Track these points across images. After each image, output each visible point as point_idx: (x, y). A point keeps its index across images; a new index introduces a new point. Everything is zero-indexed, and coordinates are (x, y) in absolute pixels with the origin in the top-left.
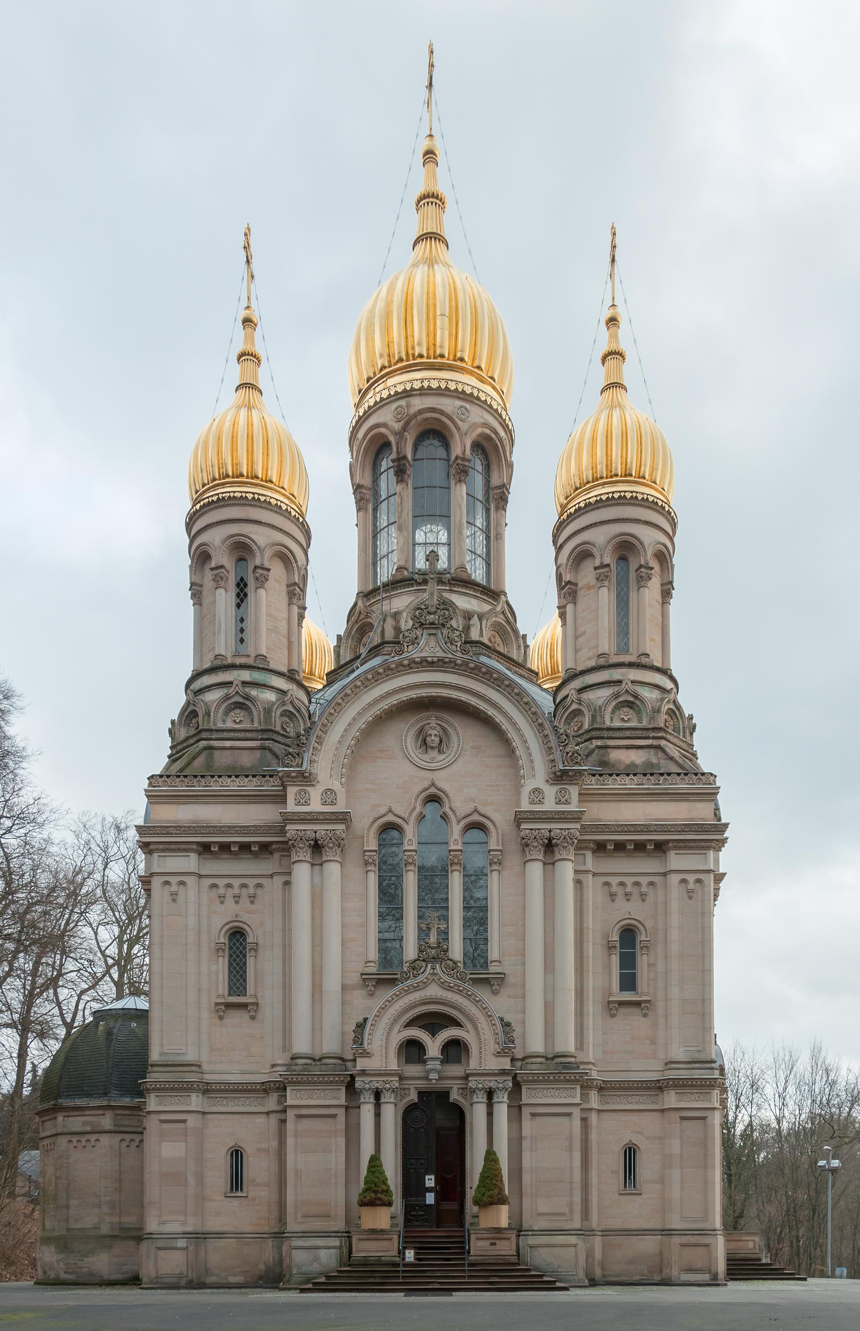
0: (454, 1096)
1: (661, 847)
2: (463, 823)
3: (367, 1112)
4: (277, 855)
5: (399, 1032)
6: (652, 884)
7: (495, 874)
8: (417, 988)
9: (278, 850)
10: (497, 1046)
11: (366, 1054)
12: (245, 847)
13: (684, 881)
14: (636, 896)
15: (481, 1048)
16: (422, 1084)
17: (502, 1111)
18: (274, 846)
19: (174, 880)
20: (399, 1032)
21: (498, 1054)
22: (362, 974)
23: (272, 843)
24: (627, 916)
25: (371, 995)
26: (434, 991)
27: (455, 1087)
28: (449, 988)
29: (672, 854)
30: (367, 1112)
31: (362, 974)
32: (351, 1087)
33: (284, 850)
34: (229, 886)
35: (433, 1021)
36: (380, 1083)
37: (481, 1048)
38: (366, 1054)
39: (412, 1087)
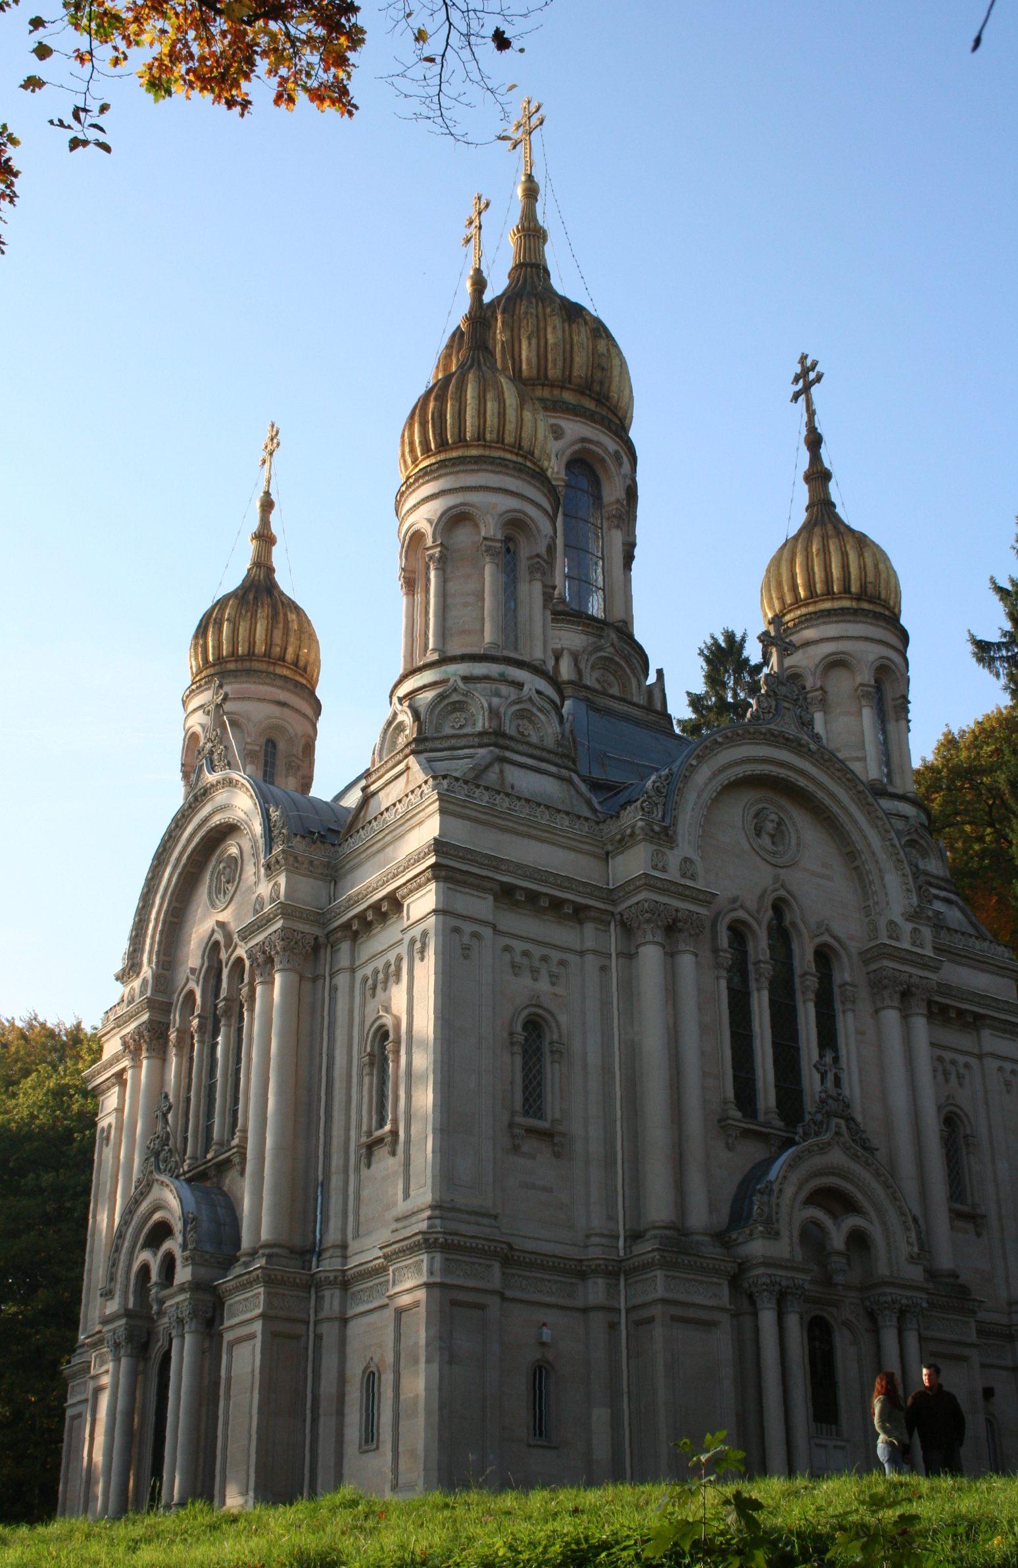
1: (972, 1022)
4: (589, 928)
6: (967, 1066)
7: (850, 1015)
8: (823, 1149)
9: (594, 920)
11: (776, 1235)
12: (556, 905)
13: (1000, 1069)
14: (953, 1078)
17: (912, 1340)
18: (593, 914)
19: (468, 928)
21: (912, 1259)
23: (588, 907)
25: (730, 1148)
26: (836, 1157)
28: (855, 1157)
29: (986, 1033)
32: (735, 1281)
33: (602, 921)
34: (526, 954)
35: (834, 1199)
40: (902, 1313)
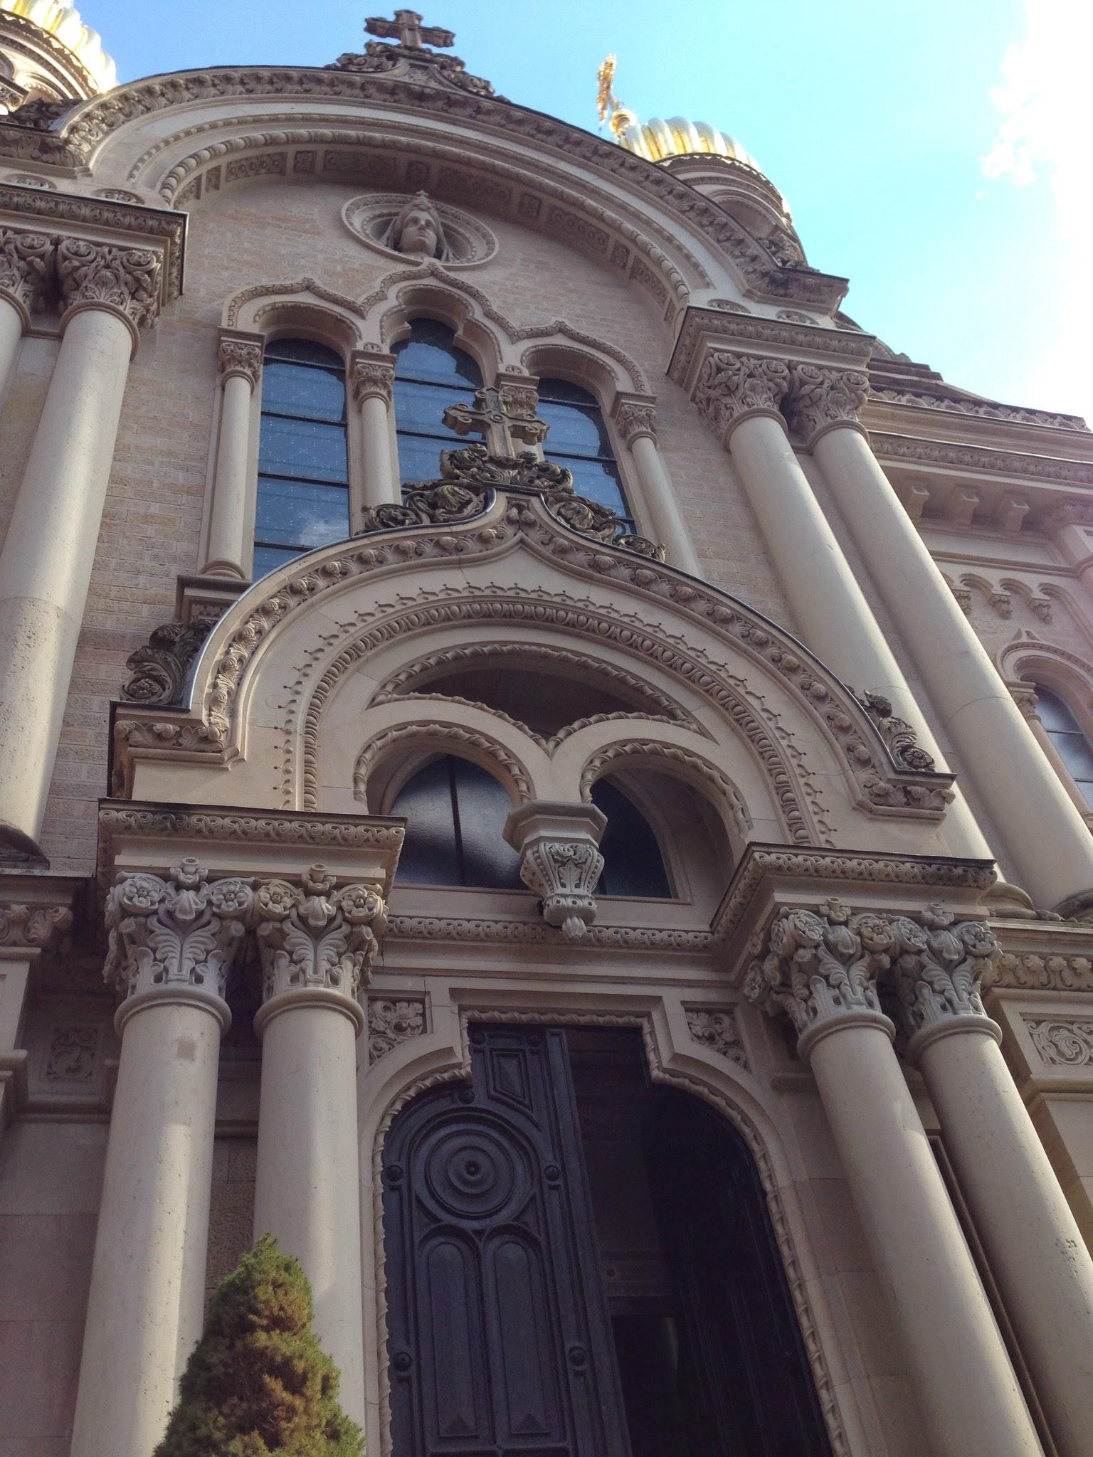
0: (673, 1042)
2: (526, 345)
3: (175, 1055)
5: (373, 703)
10: (864, 775)
15: (782, 789)
16: (495, 973)
20: (373, 703)
22: (183, 583)
24: (1024, 639)
27: (672, 999)
30: (175, 1055)
31: (183, 583)
36: (277, 886)
37: (782, 789)
38: (204, 750)
39: (439, 989)
40: (897, 990)
